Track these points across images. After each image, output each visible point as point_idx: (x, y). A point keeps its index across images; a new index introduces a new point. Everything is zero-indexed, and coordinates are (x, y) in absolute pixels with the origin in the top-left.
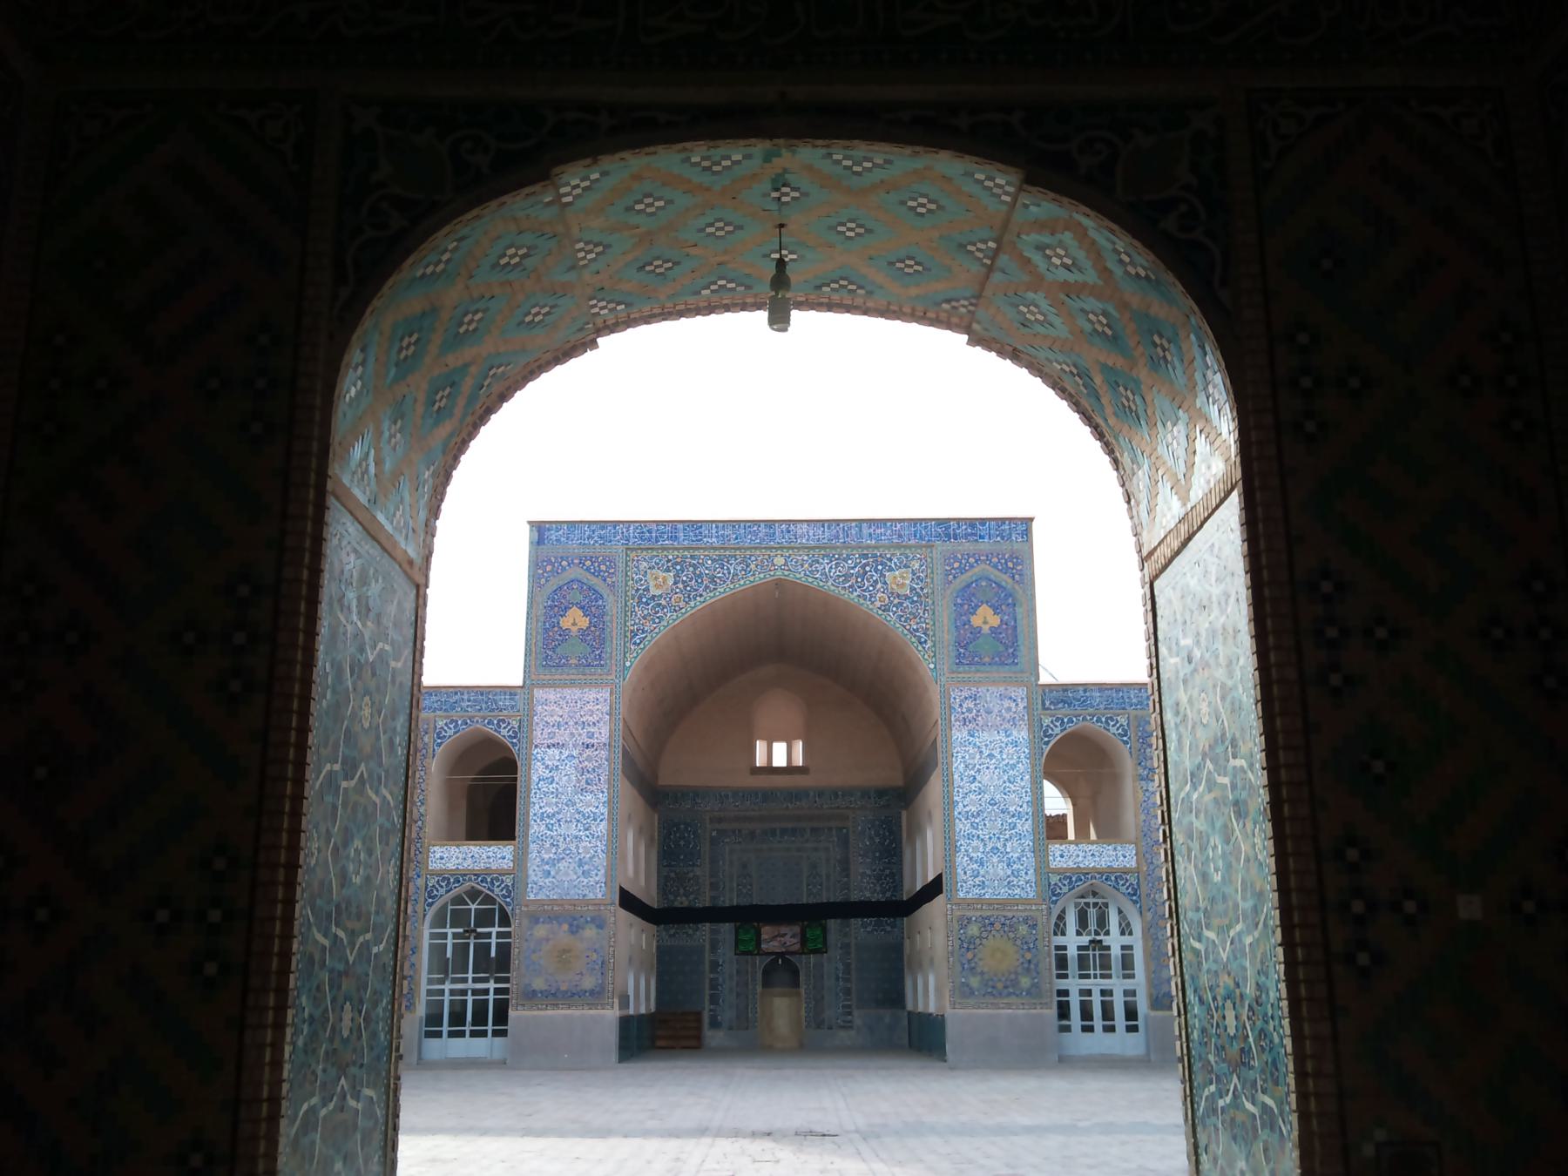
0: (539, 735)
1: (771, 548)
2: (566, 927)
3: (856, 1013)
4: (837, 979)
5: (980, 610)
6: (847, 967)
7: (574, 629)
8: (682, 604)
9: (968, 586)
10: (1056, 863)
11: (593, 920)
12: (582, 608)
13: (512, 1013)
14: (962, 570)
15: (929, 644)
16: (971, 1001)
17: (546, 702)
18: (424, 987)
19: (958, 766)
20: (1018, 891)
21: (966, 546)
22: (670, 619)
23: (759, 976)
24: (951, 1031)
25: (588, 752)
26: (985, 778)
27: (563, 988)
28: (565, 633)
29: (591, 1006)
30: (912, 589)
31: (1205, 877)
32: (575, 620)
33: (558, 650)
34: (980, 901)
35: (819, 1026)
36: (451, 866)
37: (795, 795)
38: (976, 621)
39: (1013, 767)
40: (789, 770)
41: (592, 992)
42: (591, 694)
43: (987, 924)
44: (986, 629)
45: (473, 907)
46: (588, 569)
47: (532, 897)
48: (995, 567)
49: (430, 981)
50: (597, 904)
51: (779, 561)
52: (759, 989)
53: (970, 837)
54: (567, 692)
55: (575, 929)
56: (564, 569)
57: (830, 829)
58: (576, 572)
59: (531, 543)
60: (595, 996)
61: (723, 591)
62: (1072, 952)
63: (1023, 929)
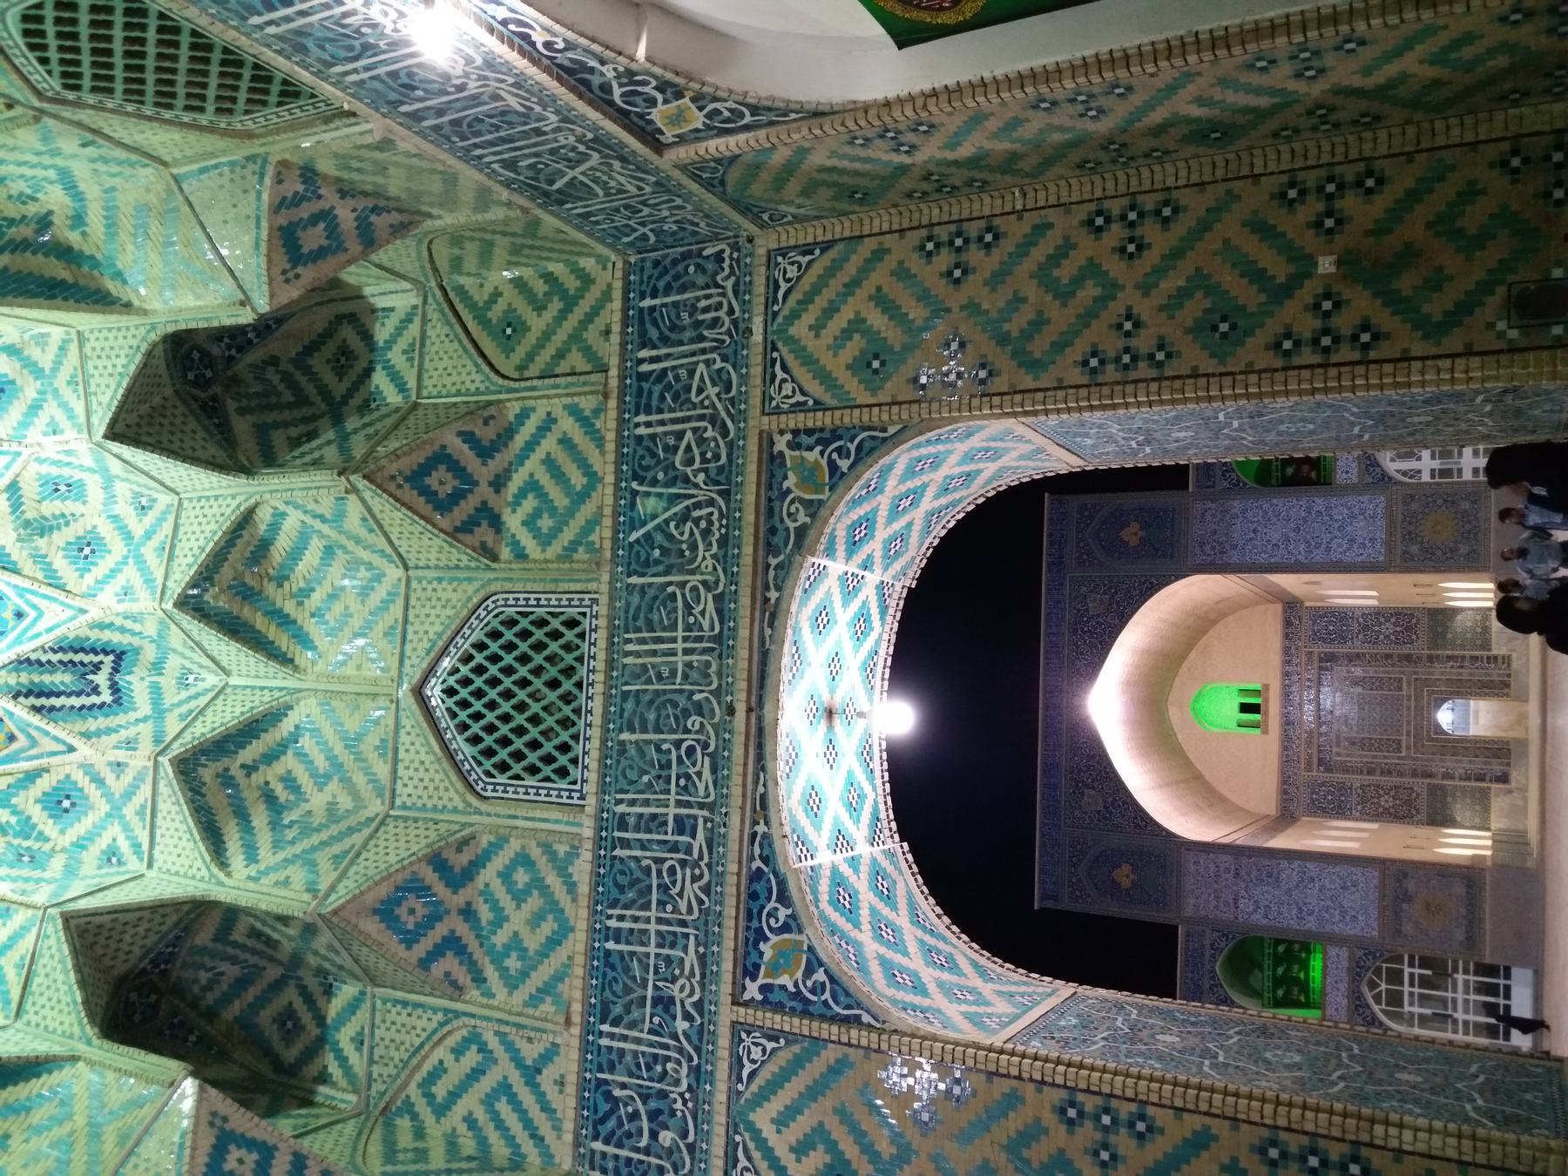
0: (1227, 915)
10: (1354, 477)
13: (1488, 960)
17: (1196, 907)
18: (1460, 1037)
27: (1463, 911)
31: (1311, 433)
34: (1389, 544)
35: (1507, 685)
36: (1345, 1002)
38: (1134, 541)
41: (1469, 886)
42: (1192, 868)
43: (1410, 537)
45: (1384, 986)
49: (1455, 1032)
50: (1382, 880)
55: (1407, 897)
62: (1436, 464)
63: (1415, 506)
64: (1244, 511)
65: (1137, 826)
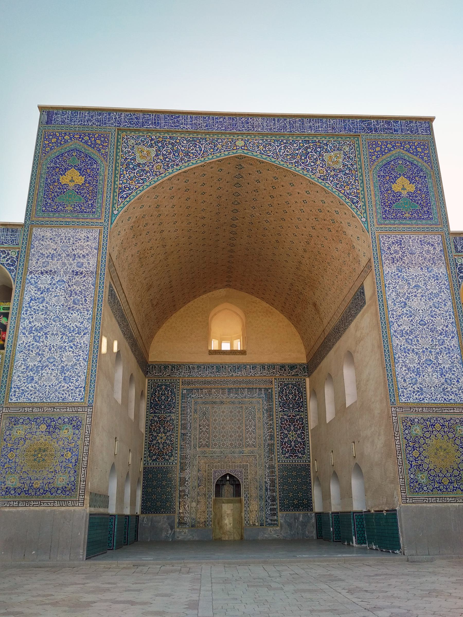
1: (234, 134)
2: (43, 427)
3: (280, 514)
4: (266, 490)
5: (398, 181)
6: (273, 481)
7: (72, 184)
8: (162, 170)
9: (389, 163)
11: (70, 421)
12: (80, 170)
14: (382, 152)
15: (361, 204)
16: (421, 496)
19: (390, 295)
20: (452, 397)
21: (385, 136)
22: (153, 181)
23: (213, 488)
24: (404, 525)
25: (77, 278)
26: (414, 303)
28: (63, 188)
29: (62, 503)
30: (344, 165)
32: (73, 178)
33: (57, 200)
34: (420, 405)
37: (238, 367)
38: (396, 187)
39: (437, 295)
40: (232, 352)
41: (64, 490)
42: (83, 234)
44: (404, 193)
46: (86, 142)
47: (14, 399)
48: (408, 151)
50: (74, 406)
51: (240, 143)
52: (213, 497)
53: (406, 351)
54: (63, 232)
56: (66, 141)
57: (260, 389)
58: (78, 144)
59: (41, 122)
60: (68, 492)
61: (194, 163)
64: (436, 278)
65: (122, 190)
